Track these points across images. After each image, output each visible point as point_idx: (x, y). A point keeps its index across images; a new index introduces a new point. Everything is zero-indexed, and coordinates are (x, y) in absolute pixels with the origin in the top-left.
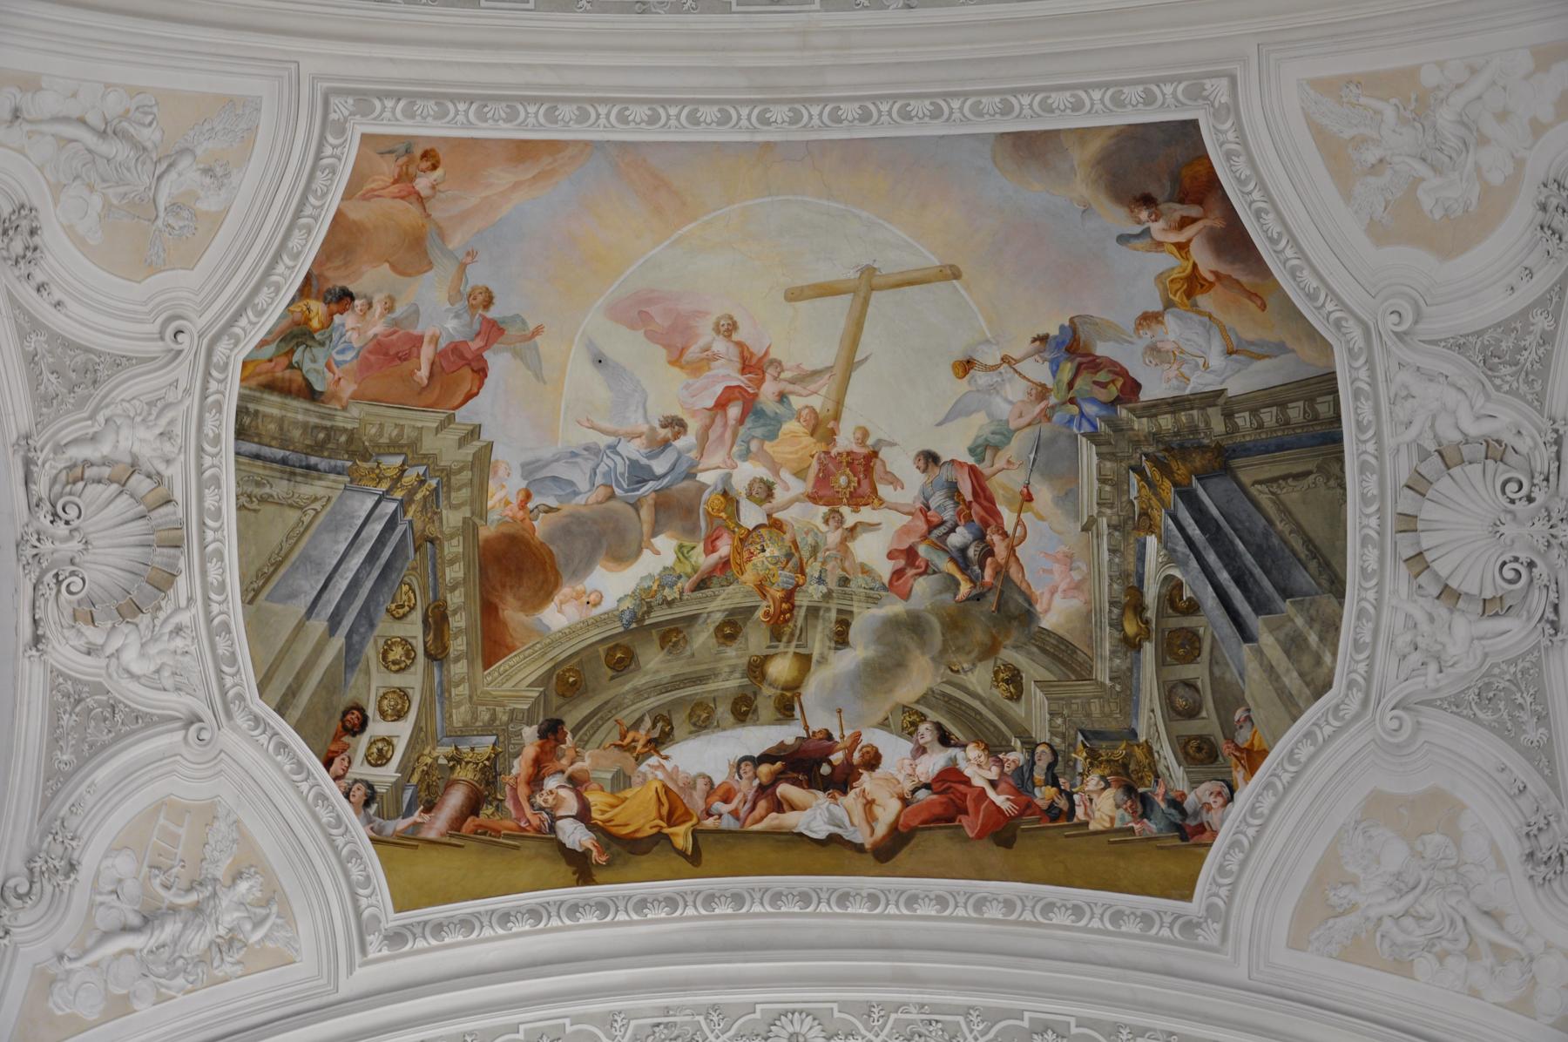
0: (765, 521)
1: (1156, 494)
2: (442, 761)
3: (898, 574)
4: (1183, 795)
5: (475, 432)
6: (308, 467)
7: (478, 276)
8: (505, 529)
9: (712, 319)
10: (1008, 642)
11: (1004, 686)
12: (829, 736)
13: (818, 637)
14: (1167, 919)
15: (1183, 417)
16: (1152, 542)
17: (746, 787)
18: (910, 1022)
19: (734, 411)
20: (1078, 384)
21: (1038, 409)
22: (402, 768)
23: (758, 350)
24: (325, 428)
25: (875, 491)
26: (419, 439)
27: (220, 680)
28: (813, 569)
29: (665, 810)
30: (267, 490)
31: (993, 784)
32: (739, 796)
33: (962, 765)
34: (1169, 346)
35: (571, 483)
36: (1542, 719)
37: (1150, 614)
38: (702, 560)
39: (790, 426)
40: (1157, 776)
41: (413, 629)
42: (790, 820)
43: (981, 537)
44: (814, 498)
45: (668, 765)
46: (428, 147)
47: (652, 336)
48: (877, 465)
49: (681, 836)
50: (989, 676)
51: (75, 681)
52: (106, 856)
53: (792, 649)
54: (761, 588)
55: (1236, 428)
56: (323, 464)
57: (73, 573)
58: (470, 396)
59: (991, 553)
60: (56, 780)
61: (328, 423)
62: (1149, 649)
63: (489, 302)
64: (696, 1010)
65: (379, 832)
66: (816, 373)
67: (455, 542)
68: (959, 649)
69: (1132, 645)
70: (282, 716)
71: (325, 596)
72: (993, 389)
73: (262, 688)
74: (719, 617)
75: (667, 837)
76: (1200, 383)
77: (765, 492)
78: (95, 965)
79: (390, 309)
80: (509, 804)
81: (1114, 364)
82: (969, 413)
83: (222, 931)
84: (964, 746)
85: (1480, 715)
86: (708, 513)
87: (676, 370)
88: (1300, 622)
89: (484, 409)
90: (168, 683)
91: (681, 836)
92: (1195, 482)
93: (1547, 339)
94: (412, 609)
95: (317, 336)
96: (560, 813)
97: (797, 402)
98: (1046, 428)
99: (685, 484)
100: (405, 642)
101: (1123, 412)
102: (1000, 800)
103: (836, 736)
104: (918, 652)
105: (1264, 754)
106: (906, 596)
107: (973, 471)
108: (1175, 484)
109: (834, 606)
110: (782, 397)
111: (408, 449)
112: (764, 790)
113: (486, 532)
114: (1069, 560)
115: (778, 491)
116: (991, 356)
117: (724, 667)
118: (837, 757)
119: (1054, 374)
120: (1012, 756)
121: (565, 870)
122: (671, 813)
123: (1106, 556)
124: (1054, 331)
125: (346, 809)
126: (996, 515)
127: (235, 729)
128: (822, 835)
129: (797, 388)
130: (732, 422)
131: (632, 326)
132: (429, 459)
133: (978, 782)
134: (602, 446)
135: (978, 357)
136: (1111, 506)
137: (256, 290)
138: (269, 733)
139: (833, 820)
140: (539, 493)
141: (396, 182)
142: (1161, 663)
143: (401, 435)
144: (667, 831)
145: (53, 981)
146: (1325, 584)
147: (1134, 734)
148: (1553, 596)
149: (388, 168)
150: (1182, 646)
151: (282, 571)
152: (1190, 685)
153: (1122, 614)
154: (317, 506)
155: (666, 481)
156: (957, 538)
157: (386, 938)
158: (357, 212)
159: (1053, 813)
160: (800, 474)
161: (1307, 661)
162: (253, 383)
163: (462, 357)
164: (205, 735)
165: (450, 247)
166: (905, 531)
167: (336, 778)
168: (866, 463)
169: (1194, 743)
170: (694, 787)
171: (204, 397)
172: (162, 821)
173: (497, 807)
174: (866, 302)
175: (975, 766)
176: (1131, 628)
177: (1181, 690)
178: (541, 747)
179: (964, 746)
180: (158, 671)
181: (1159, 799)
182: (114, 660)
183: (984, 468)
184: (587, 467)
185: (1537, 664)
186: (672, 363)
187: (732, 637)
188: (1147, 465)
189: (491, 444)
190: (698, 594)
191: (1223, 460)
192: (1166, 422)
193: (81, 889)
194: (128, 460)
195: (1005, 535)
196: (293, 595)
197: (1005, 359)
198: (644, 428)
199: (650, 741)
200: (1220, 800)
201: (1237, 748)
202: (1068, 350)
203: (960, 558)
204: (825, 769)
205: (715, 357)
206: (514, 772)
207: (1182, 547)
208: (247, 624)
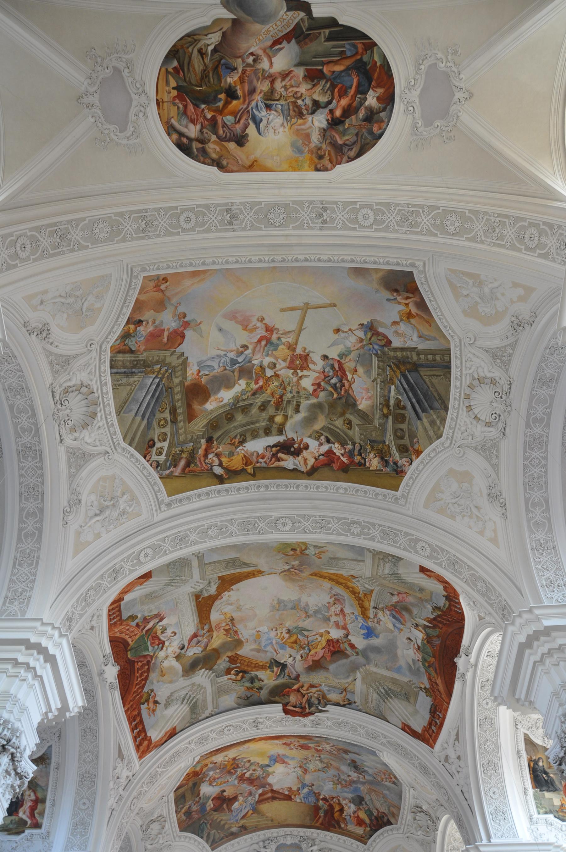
0: (273, 374)
1: (395, 374)
2: (178, 452)
3: (315, 390)
4: (398, 461)
5: (182, 354)
6: (132, 373)
7: (181, 309)
8: (193, 382)
9: (256, 317)
10: (348, 412)
11: (346, 425)
12: (293, 440)
13: (290, 410)
14: (391, 496)
15: (404, 353)
16: (393, 388)
17: (269, 454)
18: (316, 520)
19: (263, 343)
20: (373, 339)
21: (360, 345)
22: (166, 456)
23: (271, 325)
24: (137, 360)
25: (308, 366)
26: (165, 359)
27: (112, 440)
28: (288, 389)
29: (244, 462)
30: (121, 382)
31: (342, 455)
32: (267, 457)
33: (333, 449)
34: (400, 332)
35: (213, 366)
36: (498, 457)
37: (391, 408)
38: (254, 386)
39: (281, 347)
40: (391, 455)
41: (167, 415)
42: (282, 464)
43: (341, 381)
44: (289, 368)
45: (245, 449)
46: (164, 276)
47: (237, 322)
48: (309, 358)
49: (250, 469)
50: (342, 422)
51: (72, 448)
52: (88, 496)
53: (282, 413)
54: (272, 395)
55: (420, 359)
56: (136, 371)
57: (68, 420)
58: (180, 344)
59: (344, 386)
60: (72, 477)
61: (137, 359)
62: (390, 418)
63: (185, 316)
64: (255, 517)
65: (161, 475)
66: (289, 332)
67: (177, 388)
68: (333, 414)
69: (385, 416)
70: (131, 446)
71: (140, 410)
72: (346, 338)
73: (124, 439)
74: (259, 404)
75: (245, 470)
76: (410, 344)
77: (273, 366)
78: (89, 527)
79: (154, 323)
80: (198, 463)
81: (384, 334)
82: (338, 345)
83: (121, 510)
84: (334, 443)
85: (482, 453)
86: (255, 373)
87: (245, 332)
88: (435, 417)
89: (185, 347)
90: (98, 443)
91: (250, 469)
92: (407, 372)
93: (510, 355)
94: (166, 409)
95: (132, 335)
96: (214, 464)
97: (283, 340)
98: (362, 351)
99: (248, 364)
100: (164, 419)
101: (386, 349)
102: (344, 459)
103: (296, 439)
104: (321, 414)
105: (421, 452)
106: (317, 397)
107: (339, 362)
108: (401, 372)
109: (295, 400)
110: (279, 339)
111: (162, 362)
112: (274, 455)
113: (186, 384)
114: (367, 390)
115: (278, 366)
116: (346, 329)
117: (261, 419)
118: (296, 446)
119: (365, 335)
120: (348, 447)
121: (216, 480)
122: (246, 463)
123: (379, 390)
124: (366, 323)
125: (151, 470)
126: (346, 375)
127: (118, 453)
128: (291, 468)
129: (284, 336)
130: (263, 346)
131: (231, 320)
132: (169, 365)
133: (338, 454)
134: (222, 355)
135: (341, 328)
136: (381, 376)
137: (113, 327)
138: (128, 452)
139: (295, 464)
140: (203, 370)
141: (154, 288)
142: (394, 423)
143: (159, 359)
144: (245, 468)
145: (80, 533)
146: (443, 407)
147: (384, 442)
148: (504, 425)
149: (152, 284)
150: (400, 418)
151: (127, 404)
152: (402, 430)
153: (383, 407)
154: (136, 383)
155: (242, 364)
156: (334, 381)
157: (166, 505)
158: (143, 297)
159: (359, 464)
160: (284, 360)
161: (436, 428)
162: (114, 352)
163: (177, 333)
164: (110, 457)
165: (172, 302)
166: (317, 378)
167: (148, 461)
168: (305, 358)
169: (402, 447)
170: (253, 455)
171: (100, 360)
172: (101, 483)
173: (195, 465)
174: (306, 312)
175: (337, 449)
176: (385, 411)
177: (399, 431)
178: (207, 445)
179: (334, 443)
180: (94, 441)
181: (391, 462)
182: (83, 441)
183: (342, 361)
184: (217, 361)
185: (498, 442)
186: (244, 330)
187: (263, 410)
188: (393, 365)
189: (187, 358)
190: (253, 397)
191: (416, 367)
192: (399, 354)
193: (83, 509)
194: (80, 383)
195: (348, 381)
196: (130, 411)
197: (350, 330)
198: (235, 348)
199: (239, 442)
200: (408, 464)
201: (414, 449)
202: (370, 329)
203: (334, 386)
204: (292, 449)
205: (257, 328)
206: (199, 453)
207: (402, 390)
208: (118, 422)
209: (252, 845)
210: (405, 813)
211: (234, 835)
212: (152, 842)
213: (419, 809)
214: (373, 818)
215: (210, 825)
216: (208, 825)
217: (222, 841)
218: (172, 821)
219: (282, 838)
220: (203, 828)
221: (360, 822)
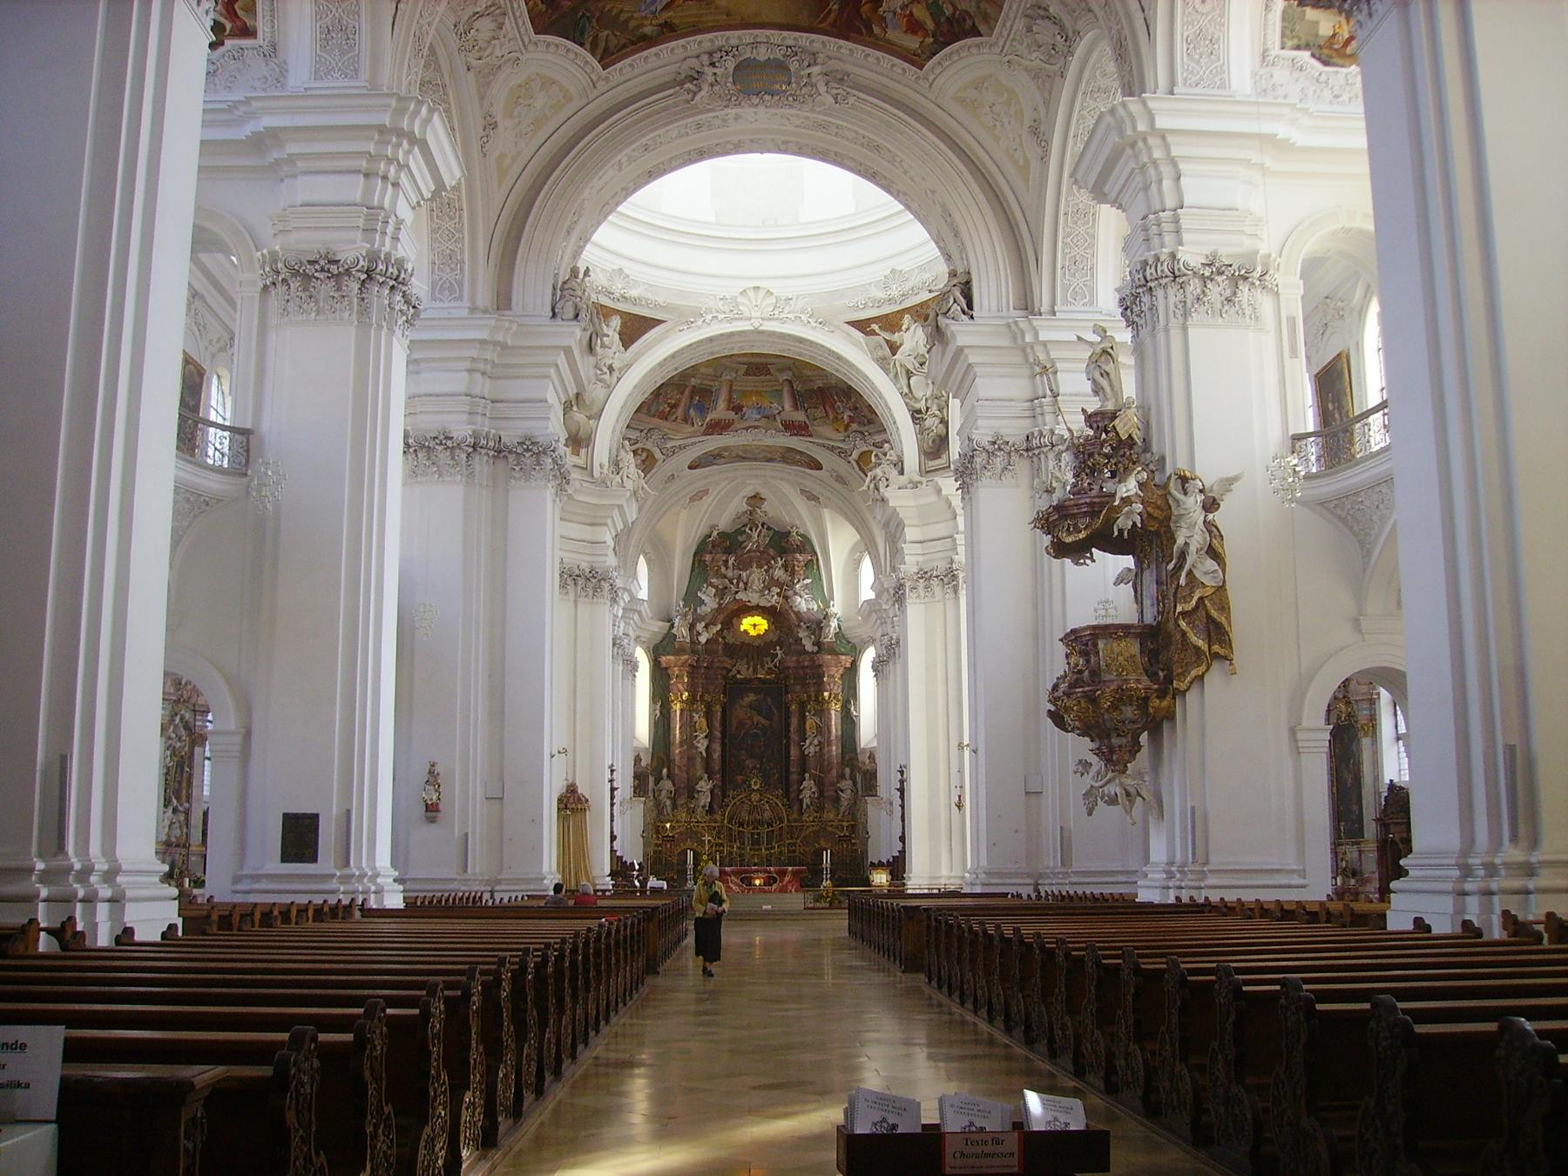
209: (685, 59)
210: (1012, 16)
211: (648, 41)
212: (479, 55)
213: (1042, 12)
214: (943, 19)
215: (598, 20)
216: (594, 21)
217: (624, 51)
218: (518, 14)
219: (749, 49)
220: (584, 27)
221: (914, 27)
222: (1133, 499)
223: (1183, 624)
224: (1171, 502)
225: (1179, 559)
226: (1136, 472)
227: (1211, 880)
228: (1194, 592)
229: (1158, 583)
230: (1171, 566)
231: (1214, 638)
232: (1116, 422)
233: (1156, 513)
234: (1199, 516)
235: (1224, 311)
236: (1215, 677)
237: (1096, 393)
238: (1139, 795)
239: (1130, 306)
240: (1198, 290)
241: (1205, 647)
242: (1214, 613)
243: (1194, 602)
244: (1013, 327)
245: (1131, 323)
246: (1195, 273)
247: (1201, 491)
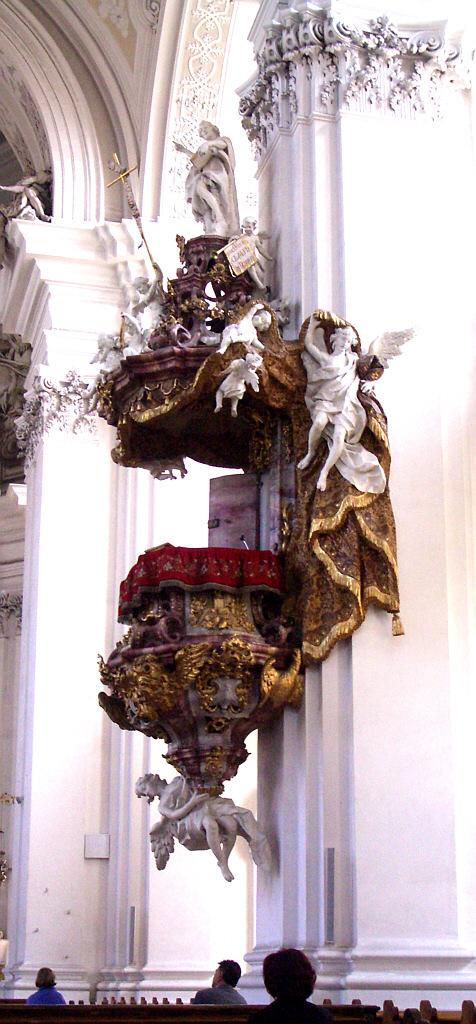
222: (248, 348)
223: (319, 551)
224: (308, 364)
225: (317, 452)
226: (254, 310)
227: (355, 976)
228: (339, 501)
229: (282, 493)
230: (304, 463)
231: (370, 576)
232: (227, 249)
233: (284, 378)
234: (349, 382)
235: (394, 101)
236: (370, 636)
237: (199, 215)
238: (241, 832)
239: (254, 108)
240: (358, 68)
241: (356, 590)
242: (371, 535)
243: (339, 515)
244: (102, 234)
245: (256, 133)
246: (354, 42)
247: (355, 349)
